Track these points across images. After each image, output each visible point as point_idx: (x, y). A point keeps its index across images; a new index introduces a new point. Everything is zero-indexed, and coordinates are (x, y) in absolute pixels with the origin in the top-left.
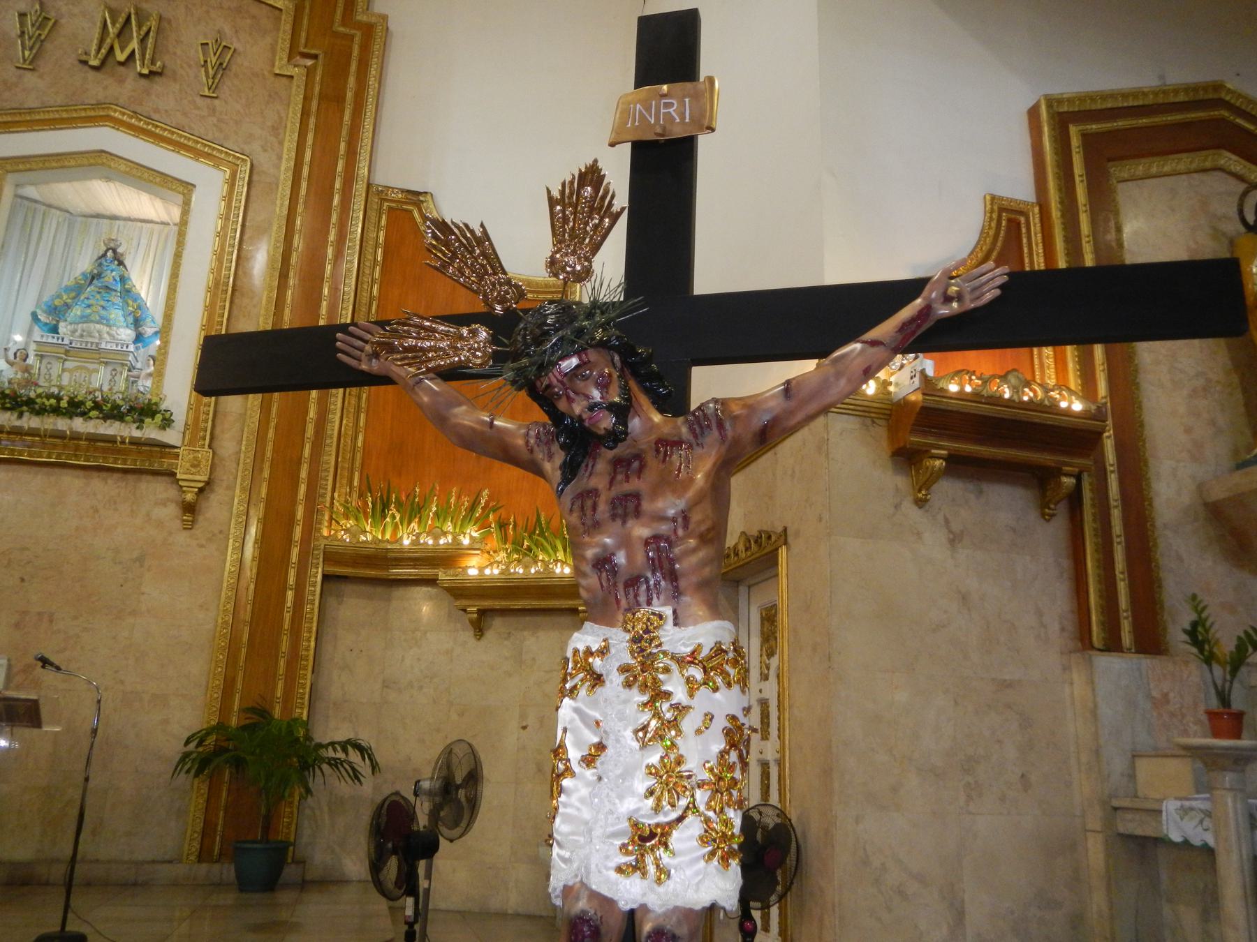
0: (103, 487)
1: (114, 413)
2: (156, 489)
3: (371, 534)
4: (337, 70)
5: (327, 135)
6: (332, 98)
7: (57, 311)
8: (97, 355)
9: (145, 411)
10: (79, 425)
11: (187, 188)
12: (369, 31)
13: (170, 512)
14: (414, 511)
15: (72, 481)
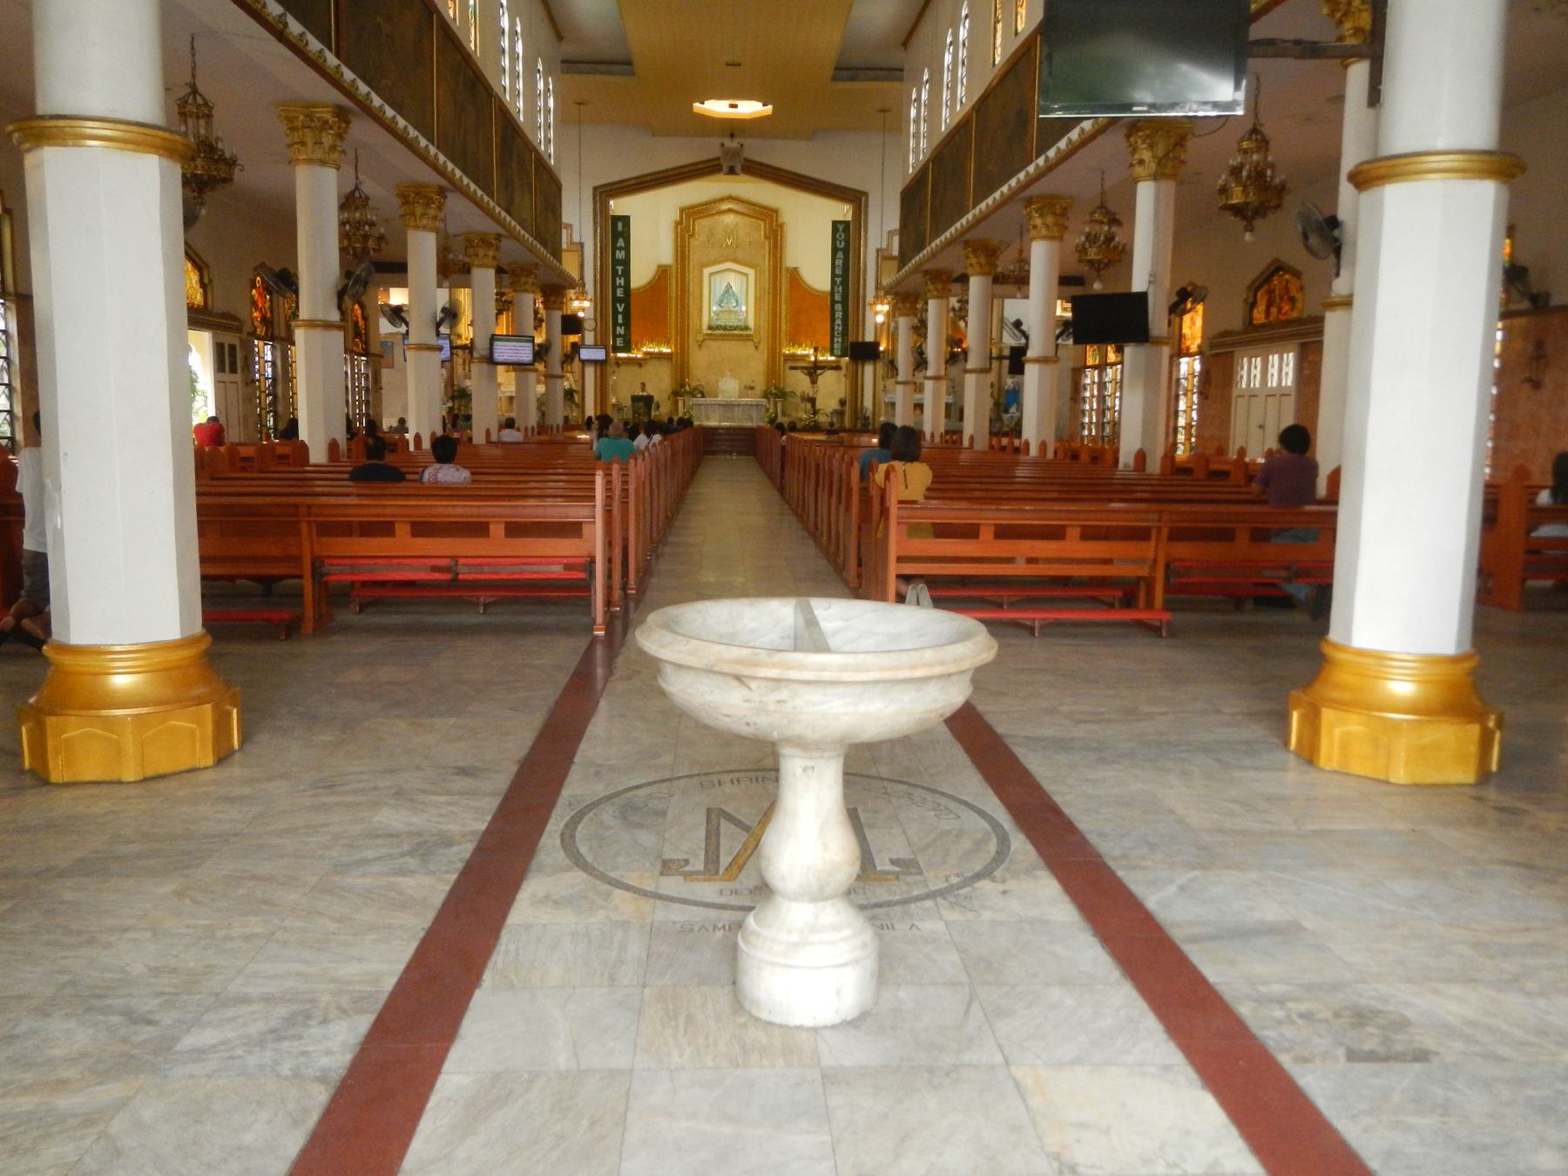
0: (739, 343)
1: (742, 330)
2: (750, 343)
3: (792, 351)
4: (776, 239)
5: (775, 256)
6: (775, 247)
7: (721, 301)
8: (732, 312)
9: (747, 328)
10: (736, 332)
11: (747, 275)
12: (783, 224)
13: (753, 348)
14: (800, 345)
15: (733, 342)
